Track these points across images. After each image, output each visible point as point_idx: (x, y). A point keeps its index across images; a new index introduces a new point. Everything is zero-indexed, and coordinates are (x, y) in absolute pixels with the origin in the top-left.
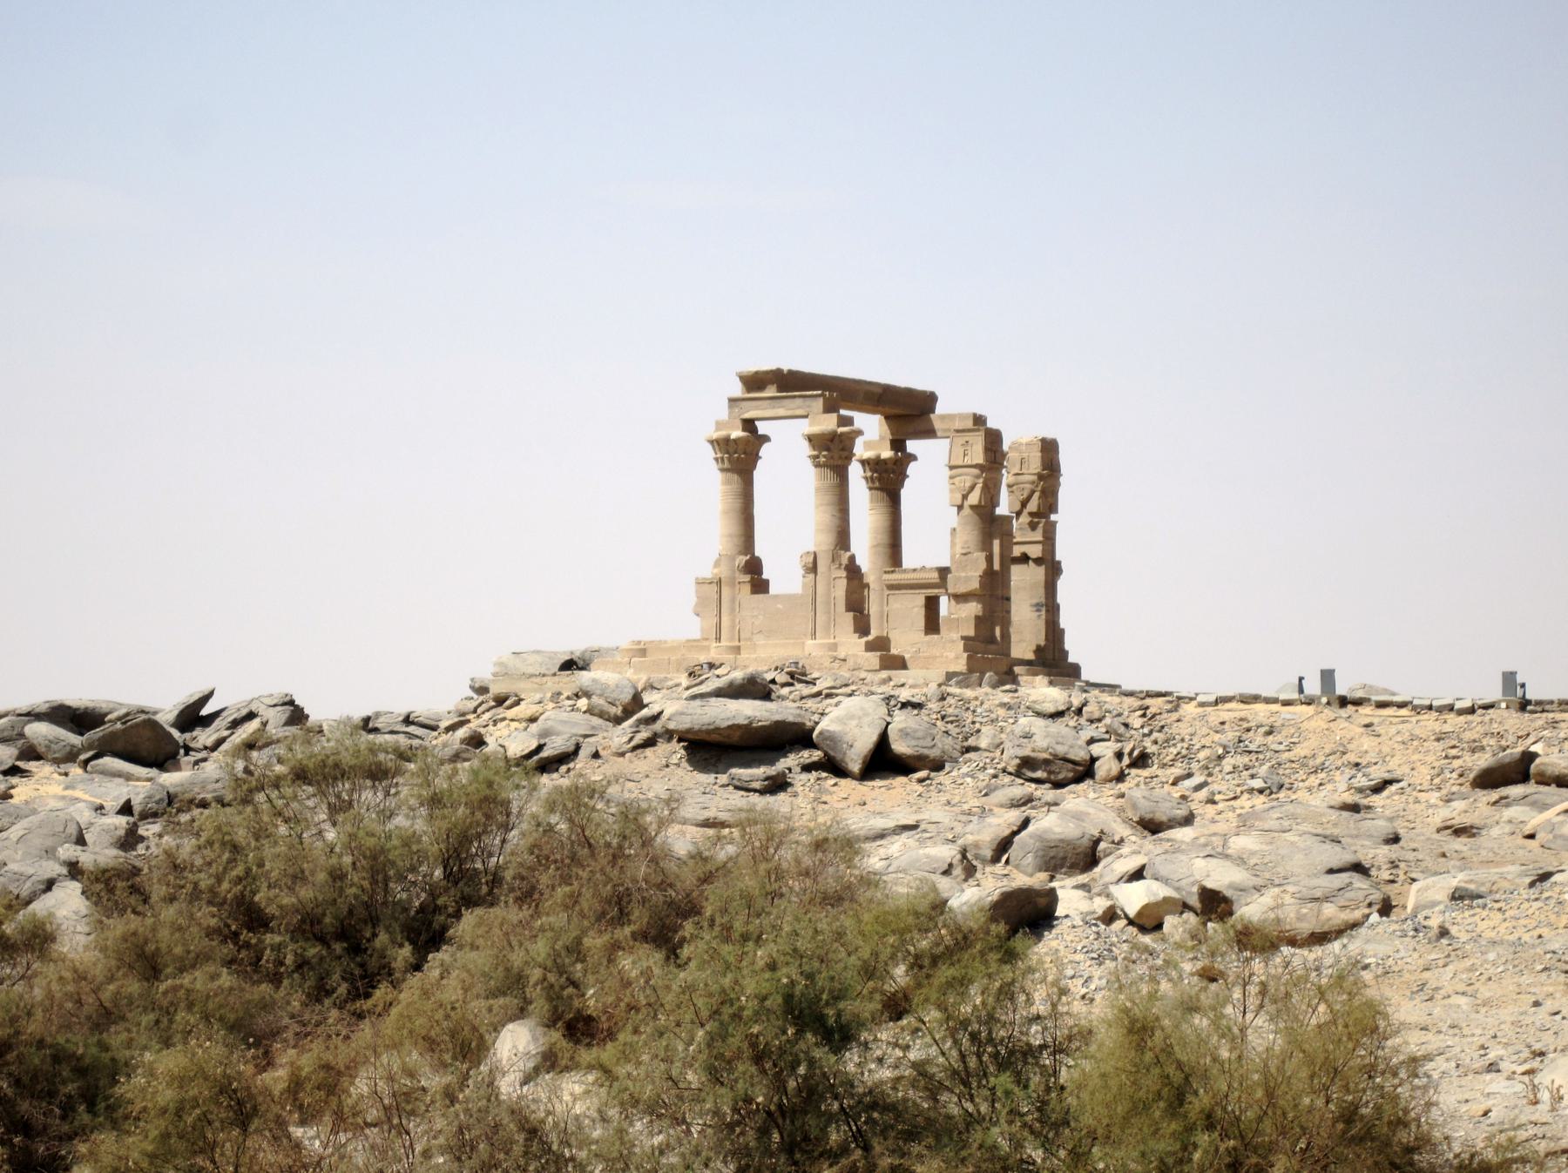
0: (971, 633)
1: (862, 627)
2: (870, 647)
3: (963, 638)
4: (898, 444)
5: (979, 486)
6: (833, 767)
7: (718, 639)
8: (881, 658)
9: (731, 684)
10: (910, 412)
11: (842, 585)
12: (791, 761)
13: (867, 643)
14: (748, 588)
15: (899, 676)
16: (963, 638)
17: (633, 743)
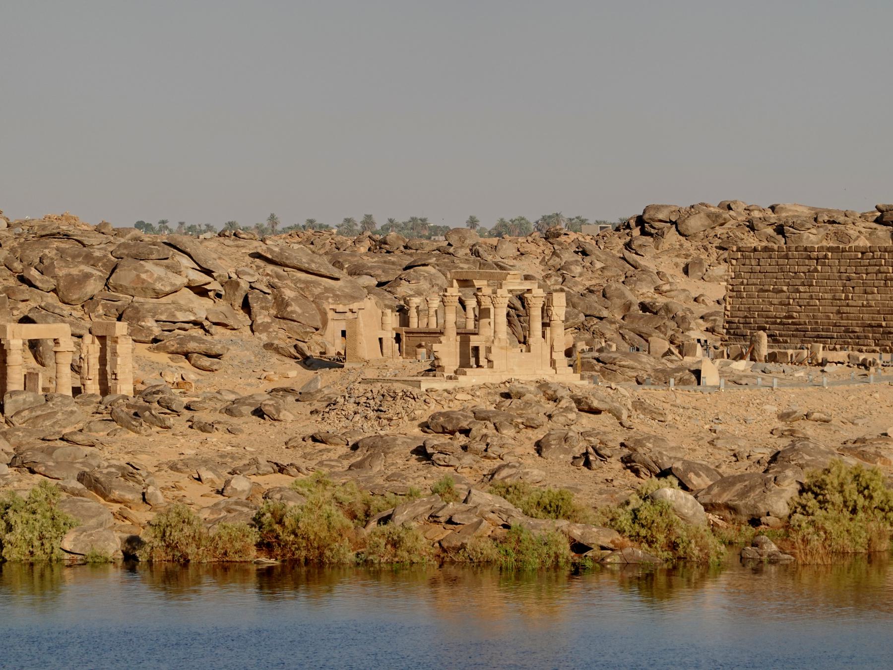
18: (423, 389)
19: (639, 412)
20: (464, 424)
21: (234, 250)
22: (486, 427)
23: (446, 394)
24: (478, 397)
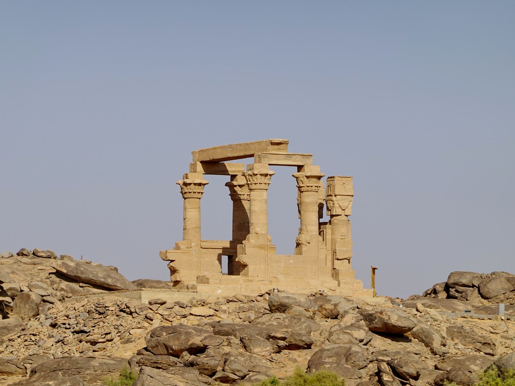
18: (145, 301)
19: (456, 341)
20: (197, 340)
21: (30, 267)
22: (229, 344)
23: (177, 308)
24: (225, 312)
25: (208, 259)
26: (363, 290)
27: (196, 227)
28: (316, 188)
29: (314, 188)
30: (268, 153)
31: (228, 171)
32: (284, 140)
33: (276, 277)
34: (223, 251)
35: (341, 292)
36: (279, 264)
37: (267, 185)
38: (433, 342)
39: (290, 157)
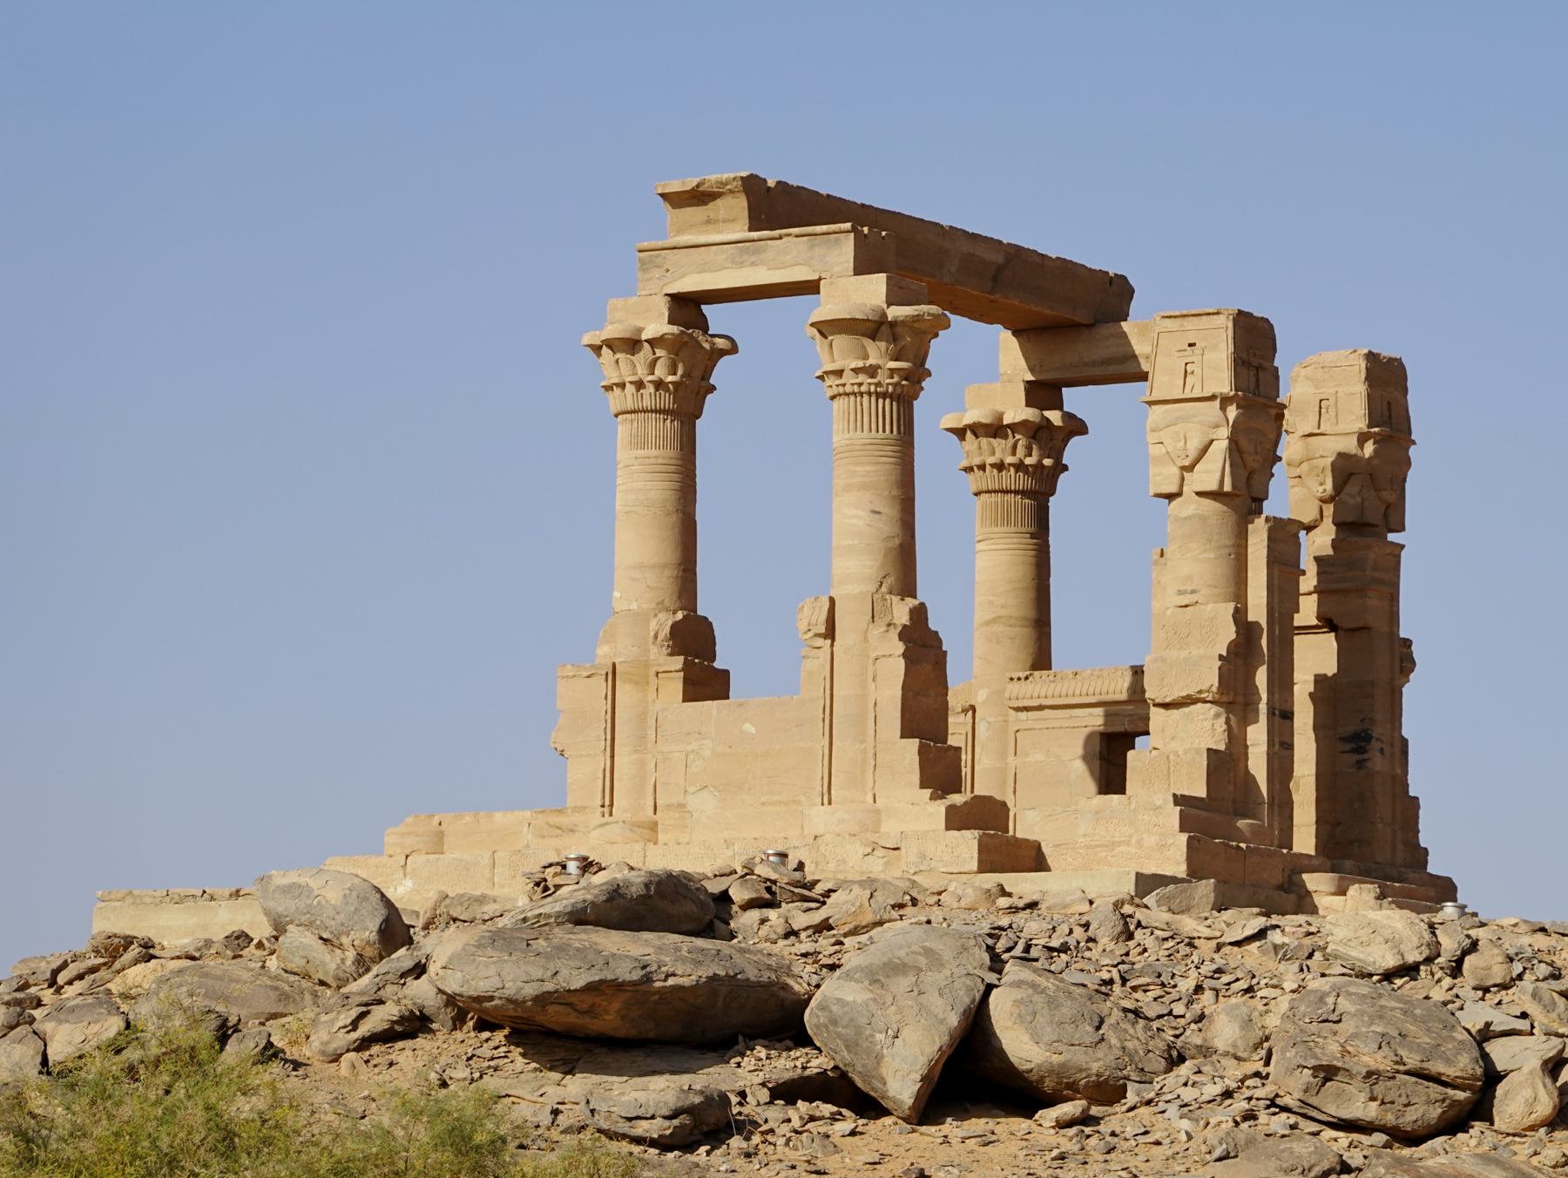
0: (1201, 791)
1: (941, 771)
2: (956, 820)
3: (1179, 800)
4: (1043, 392)
5: (1221, 446)
6: (851, 1095)
7: (609, 806)
8: (983, 848)
9: (615, 893)
10: (1071, 319)
11: (895, 669)
12: (748, 1074)
13: (951, 810)
14: (676, 686)
15: (1024, 885)
16: (1179, 800)
17: (365, 1029)
25: (1039, 757)
26: (1139, 842)
27: (994, 621)
28: (862, 378)
29: (848, 378)
30: (660, 244)
31: (1135, 357)
32: (713, 177)
33: (682, 806)
34: (1107, 715)
35: (923, 856)
36: (694, 746)
37: (630, 389)
38: (884, 1071)
39: (757, 252)
